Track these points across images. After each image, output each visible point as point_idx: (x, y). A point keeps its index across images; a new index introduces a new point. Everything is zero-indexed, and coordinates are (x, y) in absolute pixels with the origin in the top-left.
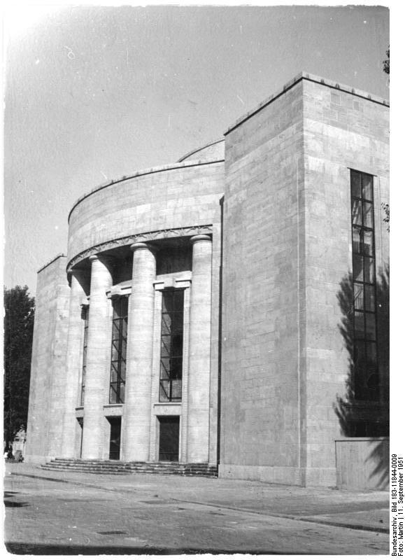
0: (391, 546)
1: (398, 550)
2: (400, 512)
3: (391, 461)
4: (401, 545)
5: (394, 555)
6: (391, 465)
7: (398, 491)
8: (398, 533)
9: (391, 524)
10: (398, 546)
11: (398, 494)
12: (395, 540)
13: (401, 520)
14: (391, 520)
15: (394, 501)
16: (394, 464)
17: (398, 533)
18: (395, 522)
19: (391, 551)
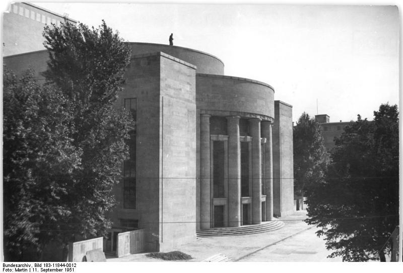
1: (7, 268)
2: (35, 270)
4: (11, 270)
5: (4, 265)
7: (50, 268)
8: (20, 268)
9: (26, 263)
10: (10, 268)
11: (47, 268)
12: (14, 266)
13: (29, 270)
14: (29, 263)
16: (69, 265)
17: (20, 268)
18: (27, 266)
19: (7, 263)
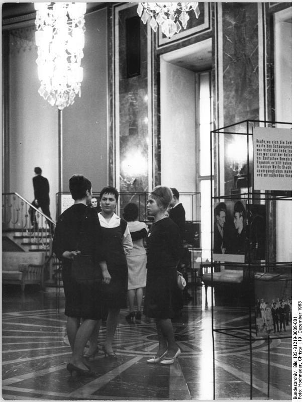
0: (293, 392)
1: (298, 395)
3: (293, 331)
4: (300, 391)
5: (295, 398)
6: (293, 333)
8: (298, 383)
9: (293, 376)
10: (298, 392)
11: (298, 355)
12: (296, 388)
14: (293, 373)
15: (296, 359)
17: (298, 383)
18: (296, 375)
19: (293, 395)
